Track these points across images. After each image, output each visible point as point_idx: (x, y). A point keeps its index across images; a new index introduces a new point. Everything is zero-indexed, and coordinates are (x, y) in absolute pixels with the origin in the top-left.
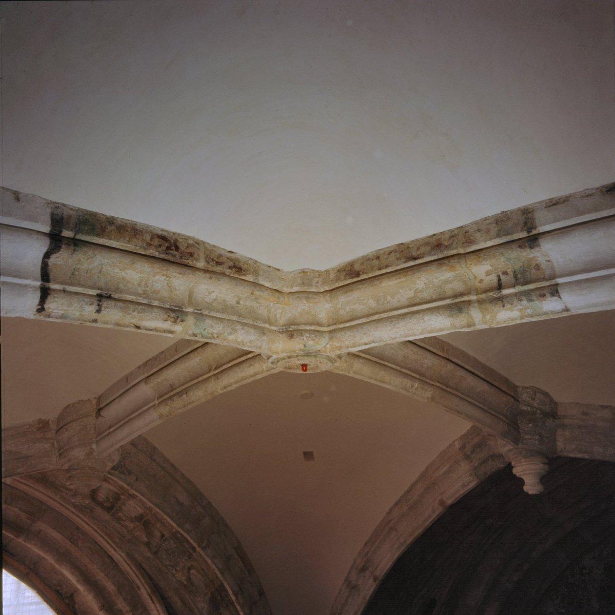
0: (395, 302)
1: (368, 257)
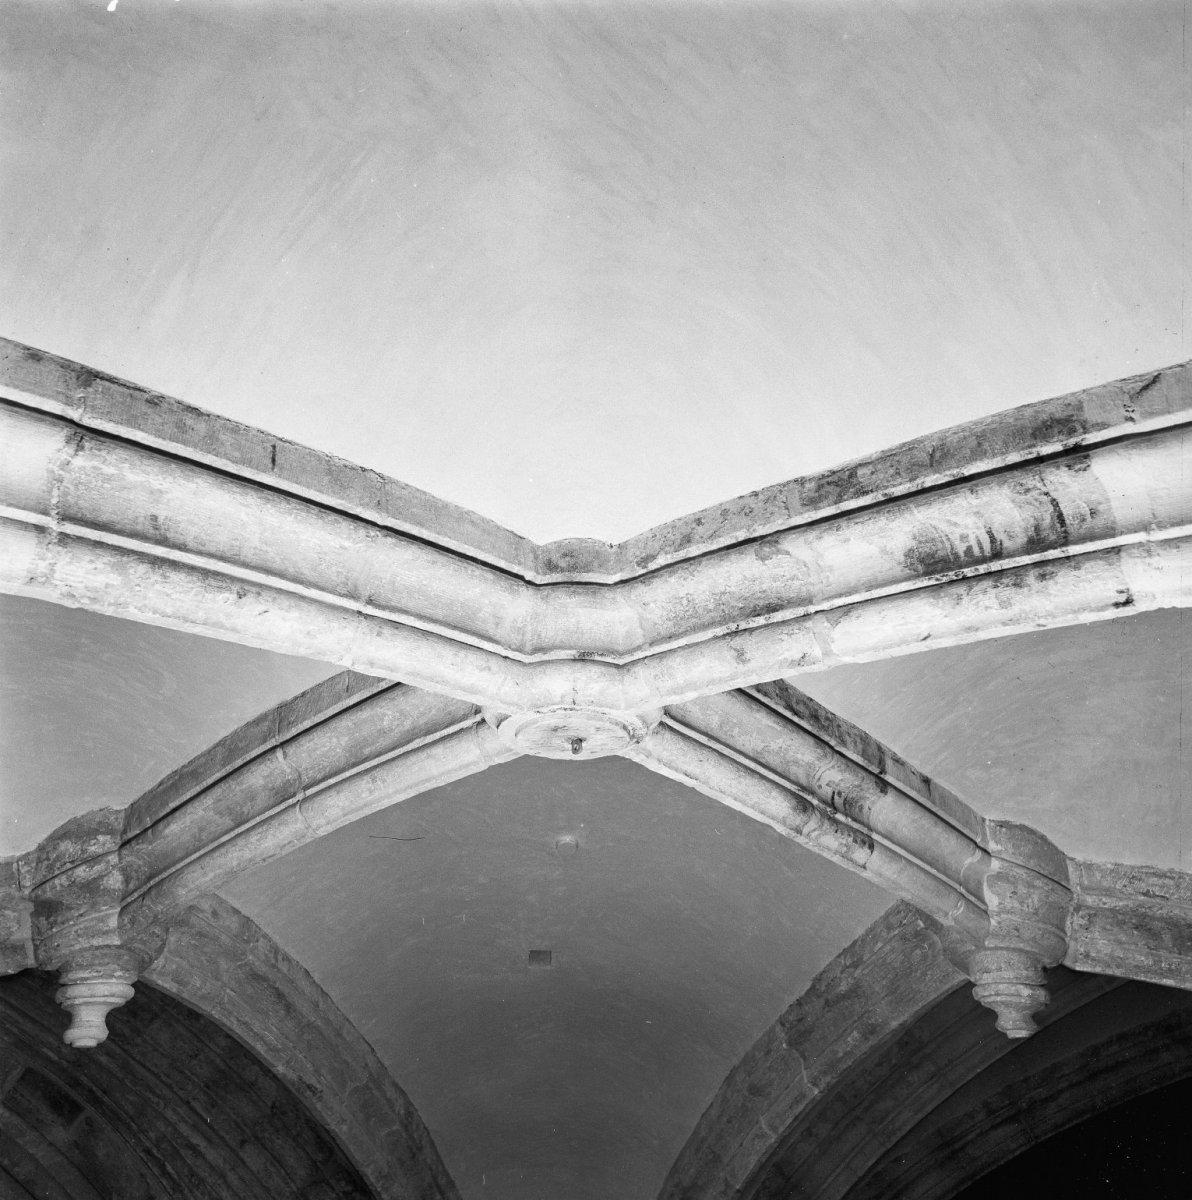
0: (741, 742)
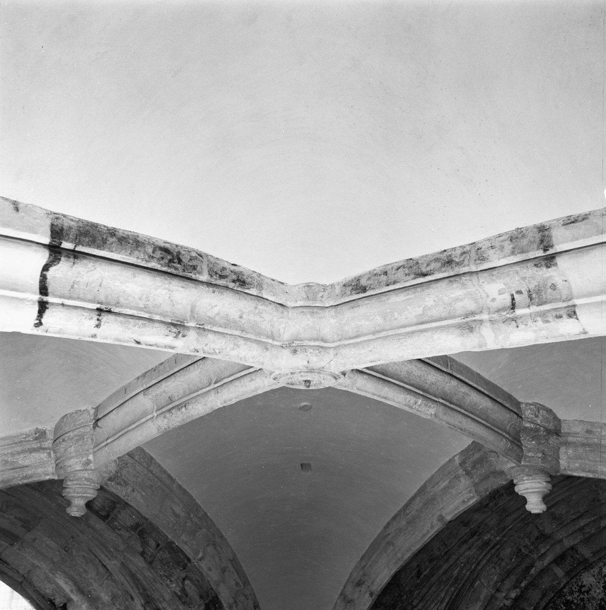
0: (402, 320)
1: (375, 272)
